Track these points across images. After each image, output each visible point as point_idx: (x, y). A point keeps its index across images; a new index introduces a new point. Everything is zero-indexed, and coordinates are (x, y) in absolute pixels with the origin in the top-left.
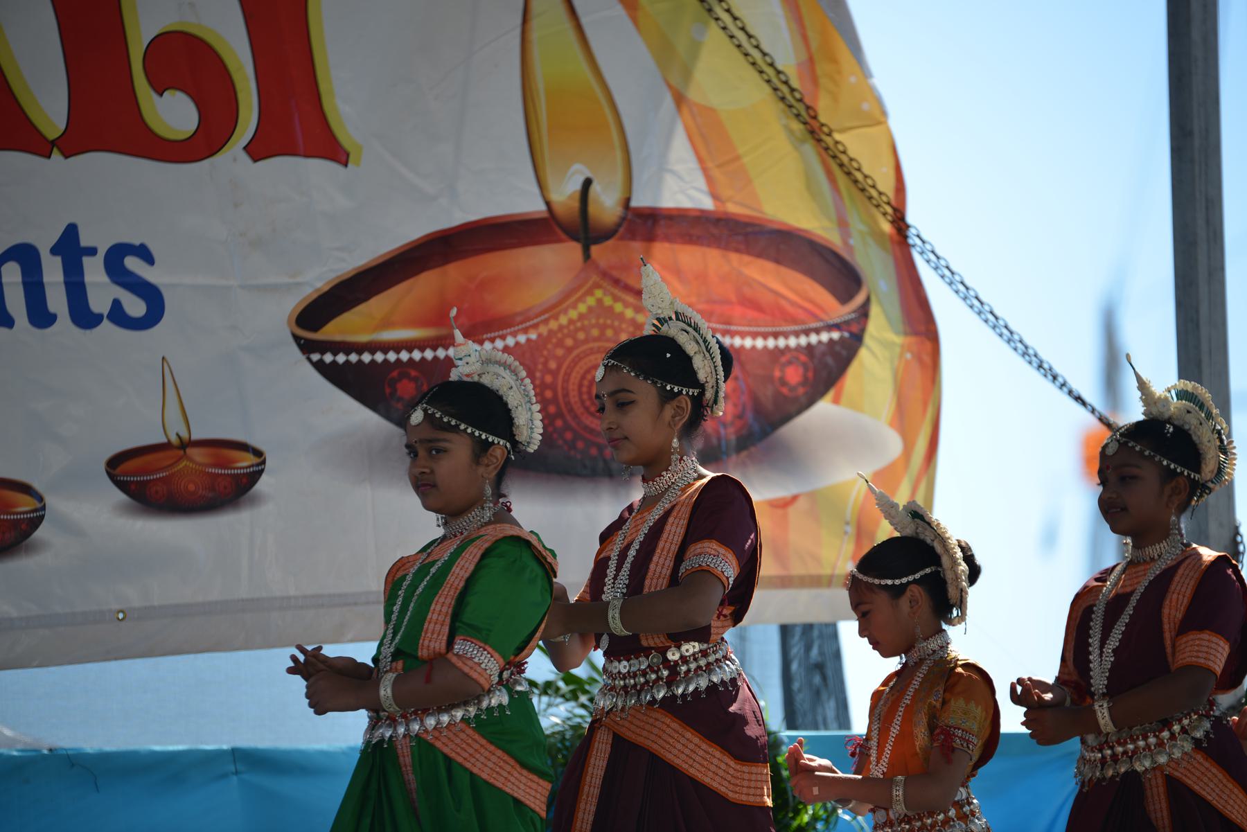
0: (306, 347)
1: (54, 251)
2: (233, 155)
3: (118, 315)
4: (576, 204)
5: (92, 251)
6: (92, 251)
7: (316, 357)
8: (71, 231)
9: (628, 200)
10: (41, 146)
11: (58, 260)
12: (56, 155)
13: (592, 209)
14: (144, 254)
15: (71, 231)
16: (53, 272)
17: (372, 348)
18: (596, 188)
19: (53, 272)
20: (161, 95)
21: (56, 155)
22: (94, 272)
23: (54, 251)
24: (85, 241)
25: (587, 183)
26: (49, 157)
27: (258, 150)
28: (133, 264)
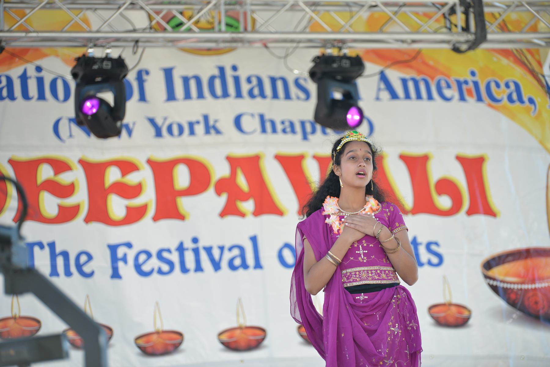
0: (486, 277)
2: (462, 214)
3: (430, 263)
5: (421, 244)
6: (421, 244)
14: (436, 244)
23: (412, 243)
27: (470, 213)
28: (434, 247)
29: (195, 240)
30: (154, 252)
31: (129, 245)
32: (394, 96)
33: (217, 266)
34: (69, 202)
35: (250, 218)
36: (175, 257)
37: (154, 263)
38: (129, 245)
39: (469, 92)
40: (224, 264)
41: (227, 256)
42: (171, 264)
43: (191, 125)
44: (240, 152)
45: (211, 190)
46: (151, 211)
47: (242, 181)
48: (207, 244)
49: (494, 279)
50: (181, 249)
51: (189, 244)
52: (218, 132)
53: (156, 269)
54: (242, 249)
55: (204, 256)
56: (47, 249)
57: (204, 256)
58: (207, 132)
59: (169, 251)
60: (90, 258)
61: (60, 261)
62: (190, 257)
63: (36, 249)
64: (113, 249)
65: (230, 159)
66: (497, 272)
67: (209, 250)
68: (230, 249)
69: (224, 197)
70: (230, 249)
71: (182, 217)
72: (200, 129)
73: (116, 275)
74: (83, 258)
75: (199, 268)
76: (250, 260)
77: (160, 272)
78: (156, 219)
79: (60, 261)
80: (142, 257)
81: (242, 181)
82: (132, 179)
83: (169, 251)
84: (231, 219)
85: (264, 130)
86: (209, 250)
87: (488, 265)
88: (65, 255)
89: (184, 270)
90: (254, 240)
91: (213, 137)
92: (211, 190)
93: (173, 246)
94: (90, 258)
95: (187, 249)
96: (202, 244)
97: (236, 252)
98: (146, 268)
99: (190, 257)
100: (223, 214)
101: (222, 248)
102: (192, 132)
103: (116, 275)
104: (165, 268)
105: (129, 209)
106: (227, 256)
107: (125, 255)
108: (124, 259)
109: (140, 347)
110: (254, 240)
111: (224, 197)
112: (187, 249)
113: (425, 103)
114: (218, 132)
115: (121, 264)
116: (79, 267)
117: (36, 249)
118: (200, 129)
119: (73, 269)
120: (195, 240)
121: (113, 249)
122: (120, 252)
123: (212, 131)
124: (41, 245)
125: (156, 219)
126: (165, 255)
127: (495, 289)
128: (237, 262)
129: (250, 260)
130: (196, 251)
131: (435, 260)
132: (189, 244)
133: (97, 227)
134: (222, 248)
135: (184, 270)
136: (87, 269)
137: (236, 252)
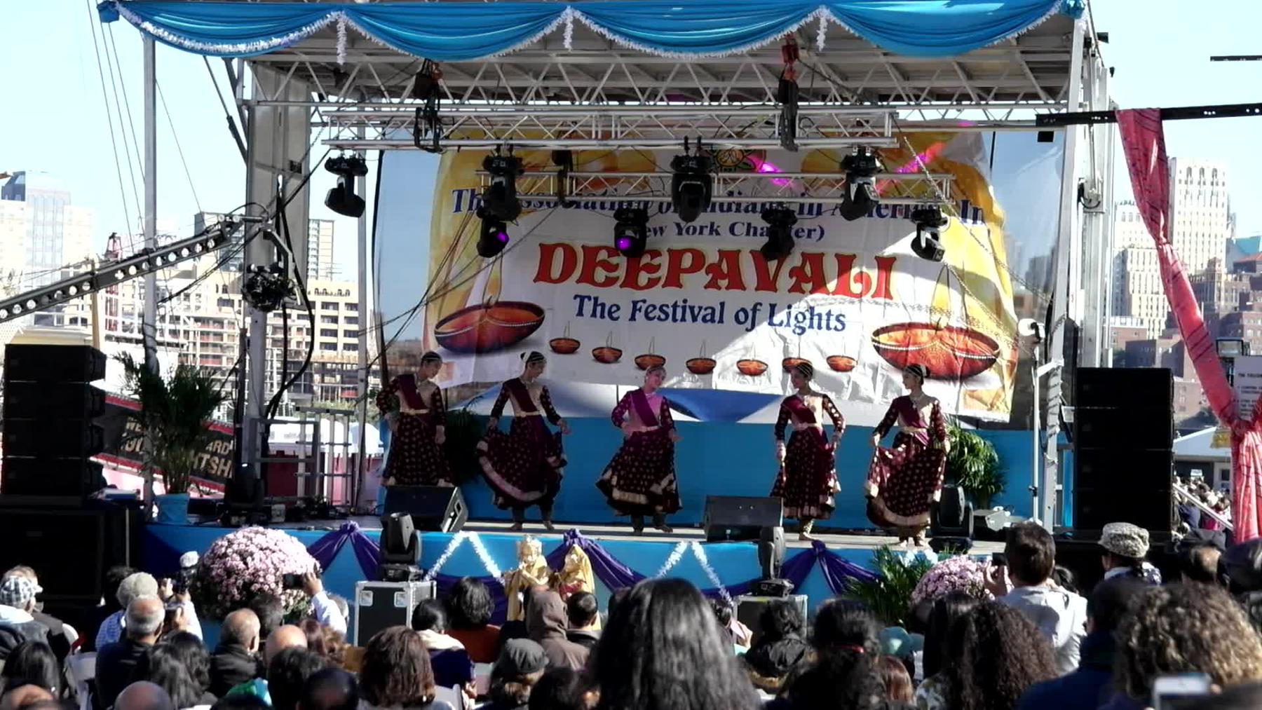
3: (836, 329)
14: (844, 316)
16: (824, 317)
19: (824, 317)
22: (833, 319)
28: (841, 318)
29: (685, 301)
30: (658, 306)
31: (644, 301)
33: (694, 319)
35: (723, 290)
36: (670, 311)
37: (657, 313)
38: (644, 301)
41: (703, 313)
42: (667, 315)
43: (702, 228)
45: (703, 271)
47: (724, 267)
48: (692, 304)
49: (879, 343)
50: (675, 306)
51: (680, 303)
52: (718, 234)
54: (713, 310)
55: (688, 311)
56: (593, 301)
57: (688, 311)
58: (711, 233)
61: (599, 309)
62: (679, 311)
63: (586, 300)
65: (720, 251)
66: (883, 338)
67: (692, 308)
68: (706, 309)
70: (706, 309)
72: (706, 231)
73: (633, 318)
74: (614, 309)
75: (683, 319)
77: (659, 319)
78: (664, 286)
79: (599, 309)
80: (651, 309)
81: (724, 267)
82: (656, 261)
83: (667, 306)
84: (712, 291)
85: (748, 234)
86: (692, 308)
87: (877, 333)
88: (603, 305)
89: (675, 320)
90: (722, 304)
93: (671, 303)
94: (618, 308)
96: (688, 304)
98: (651, 315)
99: (679, 311)
100: (706, 287)
101: (700, 308)
102: (701, 233)
103: (633, 318)
104: (663, 316)
105: (649, 279)
106: (703, 313)
108: (640, 310)
109: (637, 364)
110: (722, 304)
114: (718, 234)
116: (610, 313)
117: (586, 300)
118: (706, 231)
119: (606, 314)
120: (685, 301)
121: (635, 303)
124: (589, 298)
126: (665, 308)
127: (878, 349)
128: (708, 318)
130: (684, 308)
131: (840, 327)
132: (680, 303)
133: (628, 290)
135: (675, 320)
136: (615, 315)
137: (709, 311)
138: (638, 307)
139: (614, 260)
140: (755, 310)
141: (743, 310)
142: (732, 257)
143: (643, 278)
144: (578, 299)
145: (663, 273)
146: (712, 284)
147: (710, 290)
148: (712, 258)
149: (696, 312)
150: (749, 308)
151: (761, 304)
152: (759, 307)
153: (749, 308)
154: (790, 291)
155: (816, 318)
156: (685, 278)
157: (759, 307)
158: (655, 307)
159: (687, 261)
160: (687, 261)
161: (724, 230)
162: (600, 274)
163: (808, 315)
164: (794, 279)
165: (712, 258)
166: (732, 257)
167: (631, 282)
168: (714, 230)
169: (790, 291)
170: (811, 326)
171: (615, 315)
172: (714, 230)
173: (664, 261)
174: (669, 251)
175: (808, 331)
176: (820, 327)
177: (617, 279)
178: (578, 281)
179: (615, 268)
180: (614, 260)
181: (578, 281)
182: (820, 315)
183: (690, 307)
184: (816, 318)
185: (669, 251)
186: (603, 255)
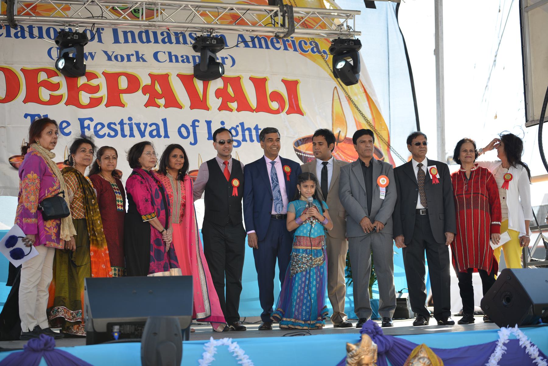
1: (254, 129)
4: (338, 135)
7: (297, 153)
8: (257, 126)
9: (346, 136)
10: (252, 110)
11: (255, 130)
12: (254, 112)
13: (339, 139)
15: (257, 126)
17: (304, 153)
18: (341, 133)
20: (272, 102)
21: (254, 112)
23: (254, 129)
24: (259, 128)
25: (340, 132)
26: (253, 112)
29: (130, 119)
31: (91, 120)
32: (247, 46)
34: (57, 93)
35: (162, 108)
36: (118, 128)
37: (106, 130)
38: (91, 120)
39: (291, 47)
40: (147, 133)
41: (149, 129)
42: (115, 131)
44: (156, 72)
45: (140, 91)
46: (105, 101)
47: (158, 88)
48: (137, 122)
50: (122, 123)
51: (126, 121)
52: (144, 60)
53: (107, 134)
54: (156, 125)
58: (138, 60)
59: (115, 124)
60: (69, 124)
64: (82, 121)
67: (138, 125)
68: (151, 125)
69: (148, 96)
70: (151, 125)
71: (123, 106)
72: (133, 58)
76: (162, 133)
77: (109, 135)
78: (107, 105)
80: (99, 127)
81: (158, 88)
82: (94, 82)
83: (115, 124)
85: (171, 61)
86: (138, 125)
89: (124, 136)
90: (164, 121)
91: (141, 63)
92: (140, 91)
94: (69, 124)
95: (126, 124)
96: (133, 122)
97: (154, 127)
98: (101, 133)
100: (146, 105)
101: (146, 125)
102: (129, 60)
104: (112, 133)
106: (149, 129)
107: (89, 125)
108: (88, 127)
110: (164, 121)
111: (148, 96)
112: (126, 124)
113: (264, 50)
114: (144, 60)
115: (86, 130)
118: (133, 58)
120: (130, 119)
121: (82, 121)
122: (86, 123)
123: (141, 60)
125: (107, 105)
126: (112, 126)
128: (155, 133)
129: (162, 133)
133: (72, 108)
134: (146, 125)
135: (124, 136)
136: (66, 131)
137: (154, 127)
138: (86, 125)
139: (54, 80)
140: (194, 126)
141: (184, 126)
142: (163, 79)
143: (84, 98)
144: (29, 118)
145: (103, 92)
146: (151, 103)
147: (150, 108)
148: (146, 81)
149: (143, 129)
150: (189, 124)
151: (198, 121)
152: (197, 124)
153: (189, 124)
154: (220, 109)
155: (247, 133)
156: (124, 97)
157: (197, 124)
158: (103, 126)
159: (123, 83)
160: (123, 83)
161: (149, 56)
162: (44, 94)
163: (239, 129)
164: (221, 99)
165: (146, 81)
166: (163, 79)
167: (73, 101)
168: (139, 58)
169: (220, 109)
170: (244, 140)
171: (66, 131)
172: (139, 58)
173: (101, 81)
174: (104, 73)
175: (243, 143)
176: (252, 140)
177: (60, 98)
178: (25, 101)
179: (56, 87)
180: (54, 80)
181: (25, 101)
182: (249, 129)
183: (136, 124)
184: (247, 133)
185: (104, 73)
186: (42, 76)
